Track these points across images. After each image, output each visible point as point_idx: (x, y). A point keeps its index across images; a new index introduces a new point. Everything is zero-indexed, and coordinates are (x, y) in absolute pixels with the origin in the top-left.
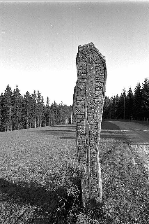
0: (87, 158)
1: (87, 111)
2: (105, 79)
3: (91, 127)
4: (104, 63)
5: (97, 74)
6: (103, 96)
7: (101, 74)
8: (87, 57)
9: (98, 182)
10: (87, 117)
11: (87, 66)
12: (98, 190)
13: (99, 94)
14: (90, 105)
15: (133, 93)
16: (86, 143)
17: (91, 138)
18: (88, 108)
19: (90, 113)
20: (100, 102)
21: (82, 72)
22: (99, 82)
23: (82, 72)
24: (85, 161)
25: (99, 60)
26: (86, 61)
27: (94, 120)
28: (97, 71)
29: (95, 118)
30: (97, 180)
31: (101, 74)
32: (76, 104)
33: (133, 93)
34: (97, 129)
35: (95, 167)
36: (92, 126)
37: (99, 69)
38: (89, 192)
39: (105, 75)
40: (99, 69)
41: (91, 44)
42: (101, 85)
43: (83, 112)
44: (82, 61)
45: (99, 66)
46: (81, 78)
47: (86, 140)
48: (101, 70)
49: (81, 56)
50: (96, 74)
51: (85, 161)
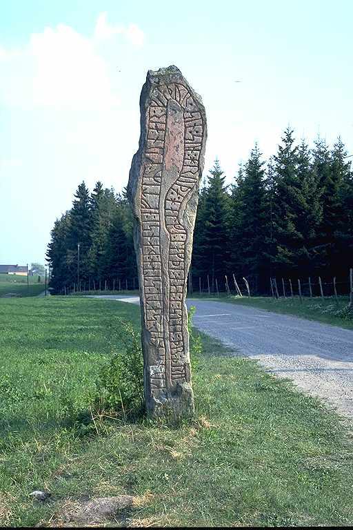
1: (165, 207)
3: (173, 239)
4: (201, 110)
5: (188, 132)
6: (197, 178)
8: (169, 97)
14: (172, 193)
18: (166, 199)
19: (172, 209)
23: (156, 126)
24: (159, 309)
25: (191, 105)
26: (166, 105)
27: (180, 224)
29: (181, 221)
30: (183, 346)
34: (185, 242)
35: (178, 321)
37: (192, 123)
39: (204, 135)
40: (192, 123)
43: (157, 209)
47: (162, 265)
48: (195, 125)
49: (153, 93)
50: (185, 132)
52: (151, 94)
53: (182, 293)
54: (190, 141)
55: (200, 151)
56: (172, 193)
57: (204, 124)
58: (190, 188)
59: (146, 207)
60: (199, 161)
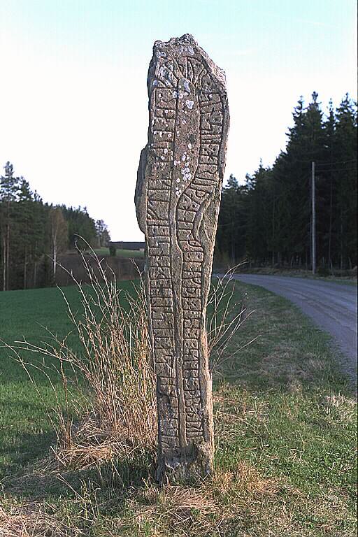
0: (176, 340)
2: (223, 135)
7: (213, 121)
8: (179, 74)
9: (203, 401)
10: (177, 232)
11: (177, 99)
12: (203, 425)
13: (208, 171)
15: (286, 152)
16: (174, 301)
17: (187, 287)
19: (185, 221)
20: (211, 194)
21: (164, 114)
22: (210, 141)
23: (164, 114)
24: (170, 348)
27: (195, 240)
28: (204, 111)
31: (213, 121)
32: (147, 197)
33: (286, 152)
35: (194, 364)
36: (189, 257)
38: (179, 429)
39: (225, 125)
41: (186, 40)
42: (214, 150)
44: (164, 86)
45: (210, 99)
46: (161, 130)
47: (173, 293)
51: (170, 348)
53: (199, 328)
54: (206, 132)
55: (220, 144)
56: (185, 200)
57: (225, 110)
58: (207, 192)
59: (153, 218)
60: (218, 157)
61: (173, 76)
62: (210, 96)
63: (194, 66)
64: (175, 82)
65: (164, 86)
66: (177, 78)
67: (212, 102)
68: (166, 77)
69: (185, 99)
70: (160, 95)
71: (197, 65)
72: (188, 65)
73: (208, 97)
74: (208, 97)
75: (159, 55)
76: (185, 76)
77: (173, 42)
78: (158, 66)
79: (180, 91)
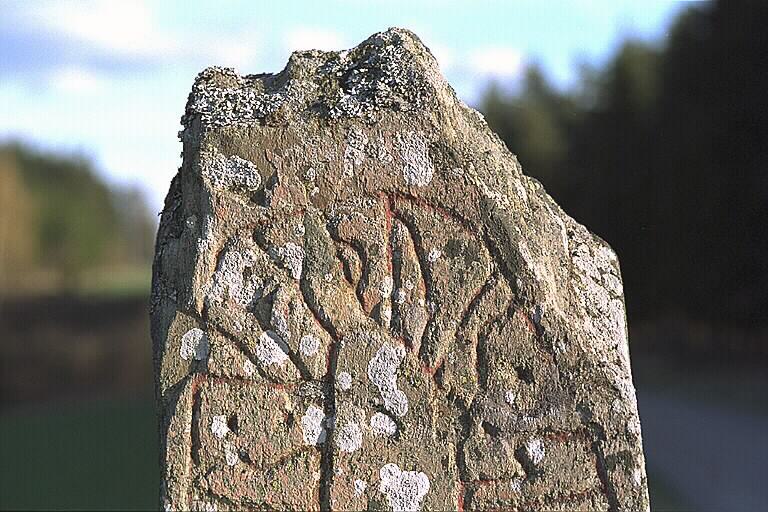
11: (326, 450)
44: (248, 368)
45: (532, 471)
52: (202, 289)
61: (301, 308)
62: (534, 448)
63: (435, 254)
64: (314, 346)
65: (248, 368)
66: (328, 326)
67: (541, 488)
68: (262, 309)
69: (371, 457)
70: (221, 427)
71: (451, 249)
72: (396, 252)
73: (521, 454)
74: (521, 454)
75: (218, 172)
76: (376, 314)
77: (305, 89)
78: (212, 241)
79: (344, 408)
